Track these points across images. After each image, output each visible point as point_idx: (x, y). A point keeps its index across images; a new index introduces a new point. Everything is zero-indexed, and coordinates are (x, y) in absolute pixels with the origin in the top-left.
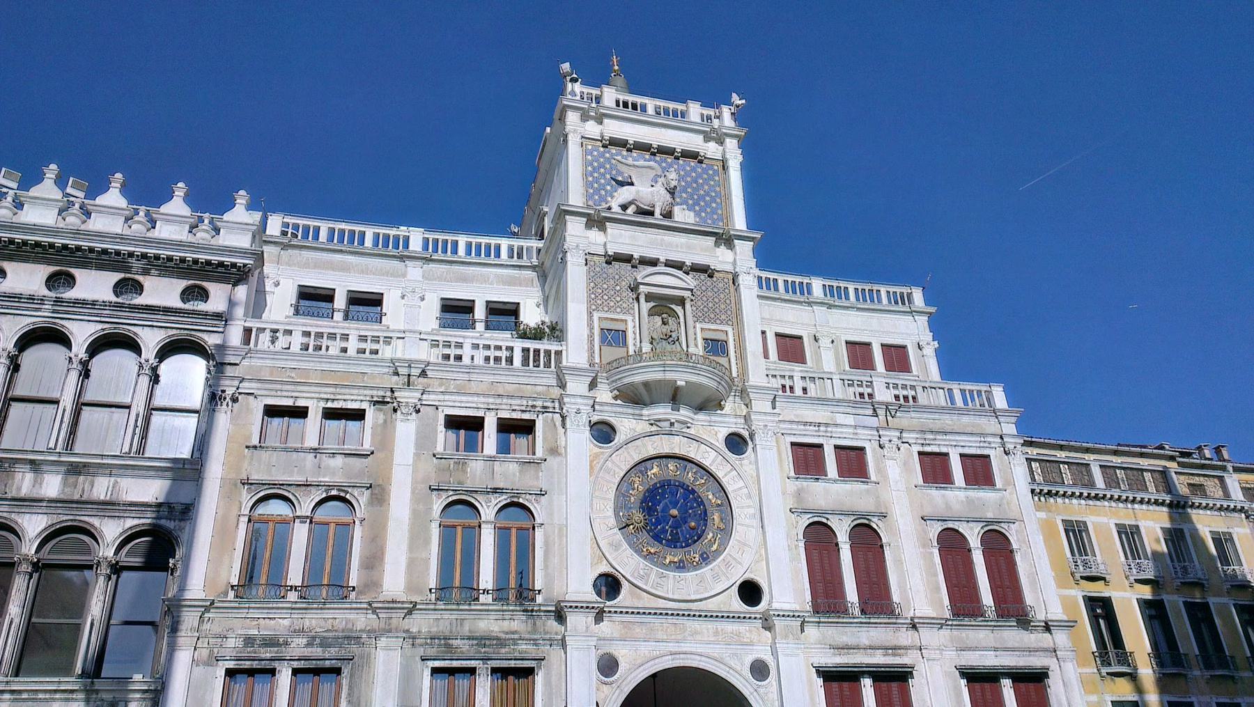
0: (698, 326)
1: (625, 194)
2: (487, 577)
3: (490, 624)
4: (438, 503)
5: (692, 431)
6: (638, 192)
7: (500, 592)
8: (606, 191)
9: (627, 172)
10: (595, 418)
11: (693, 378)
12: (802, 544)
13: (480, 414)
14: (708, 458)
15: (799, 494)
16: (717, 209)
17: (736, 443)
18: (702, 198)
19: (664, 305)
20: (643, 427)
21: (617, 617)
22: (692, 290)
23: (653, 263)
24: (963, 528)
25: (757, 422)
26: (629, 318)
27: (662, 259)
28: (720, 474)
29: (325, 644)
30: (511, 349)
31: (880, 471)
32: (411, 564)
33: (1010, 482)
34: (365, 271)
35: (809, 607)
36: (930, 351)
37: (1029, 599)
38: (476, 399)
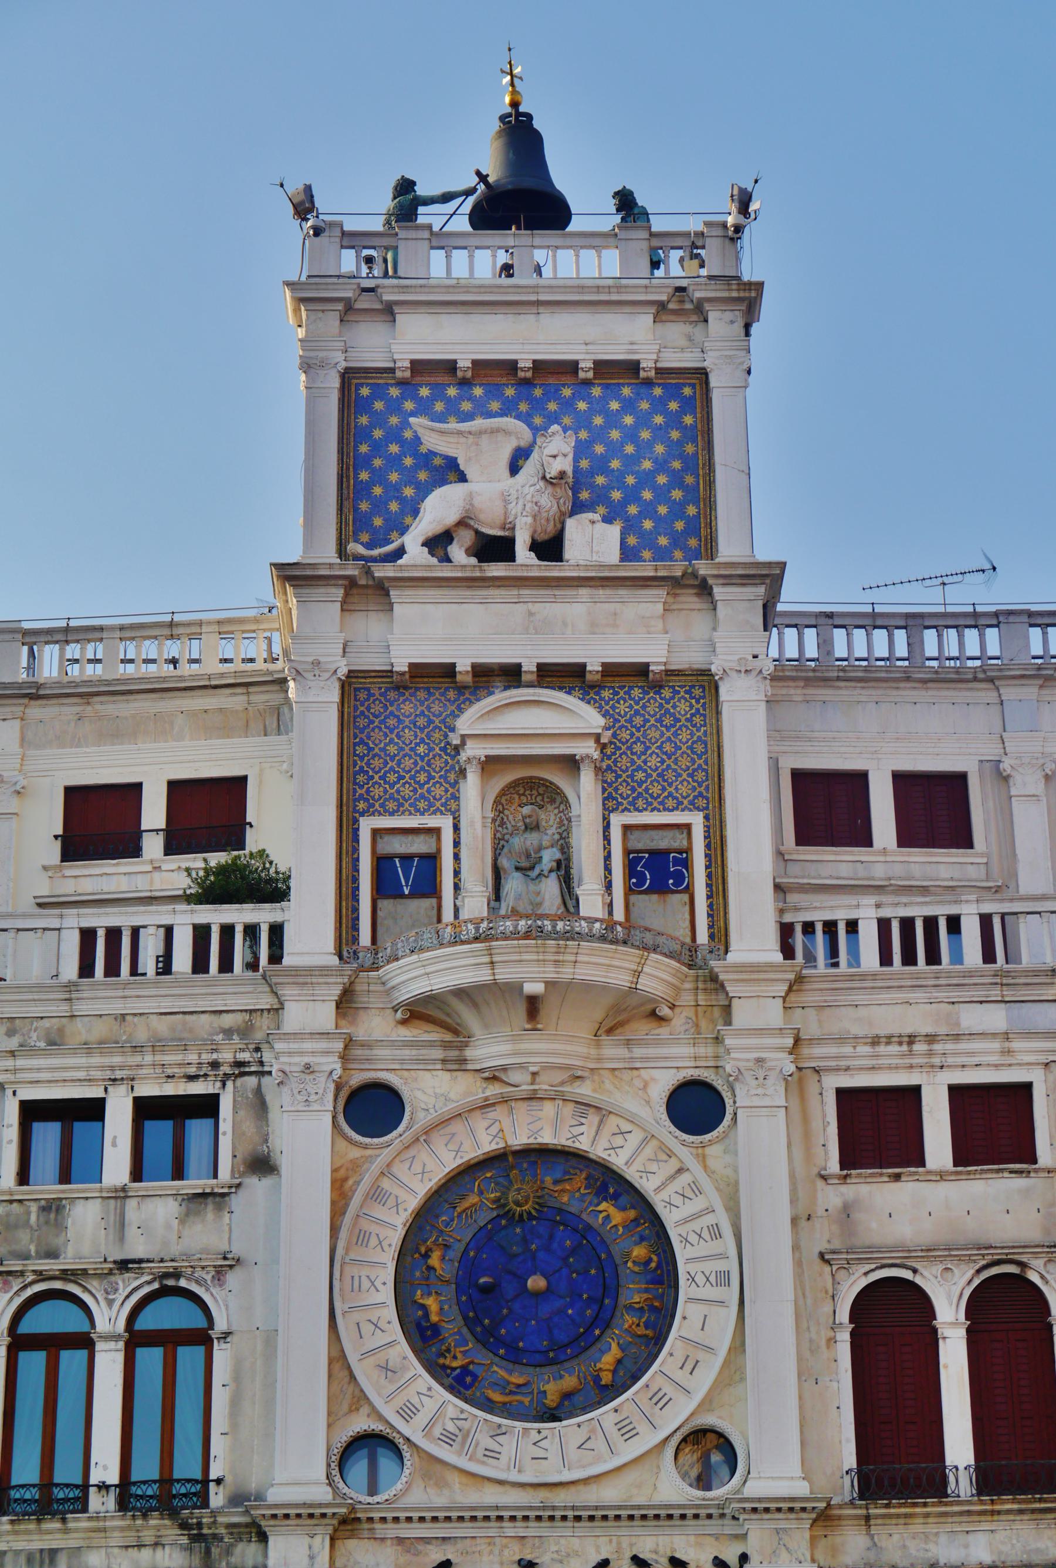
0: (617, 820)
1: (440, 508)
5: (584, 1090)
6: (471, 495)
8: (402, 500)
10: (357, 1079)
11: (567, 973)
12: (844, 1337)
13: (96, 1092)
15: (847, 1210)
16: (682, 505)
17: (697, 1107)
18: (646, 480)
19: (531, 787)
21: (392, 1531)
22: (597, 737)
23: (511, 674)
25: (739, 1051)
26: (445, 823)
27: (529, 667)
28: (647, 1186)
35: (847, 1488)
38: (82, 1061)
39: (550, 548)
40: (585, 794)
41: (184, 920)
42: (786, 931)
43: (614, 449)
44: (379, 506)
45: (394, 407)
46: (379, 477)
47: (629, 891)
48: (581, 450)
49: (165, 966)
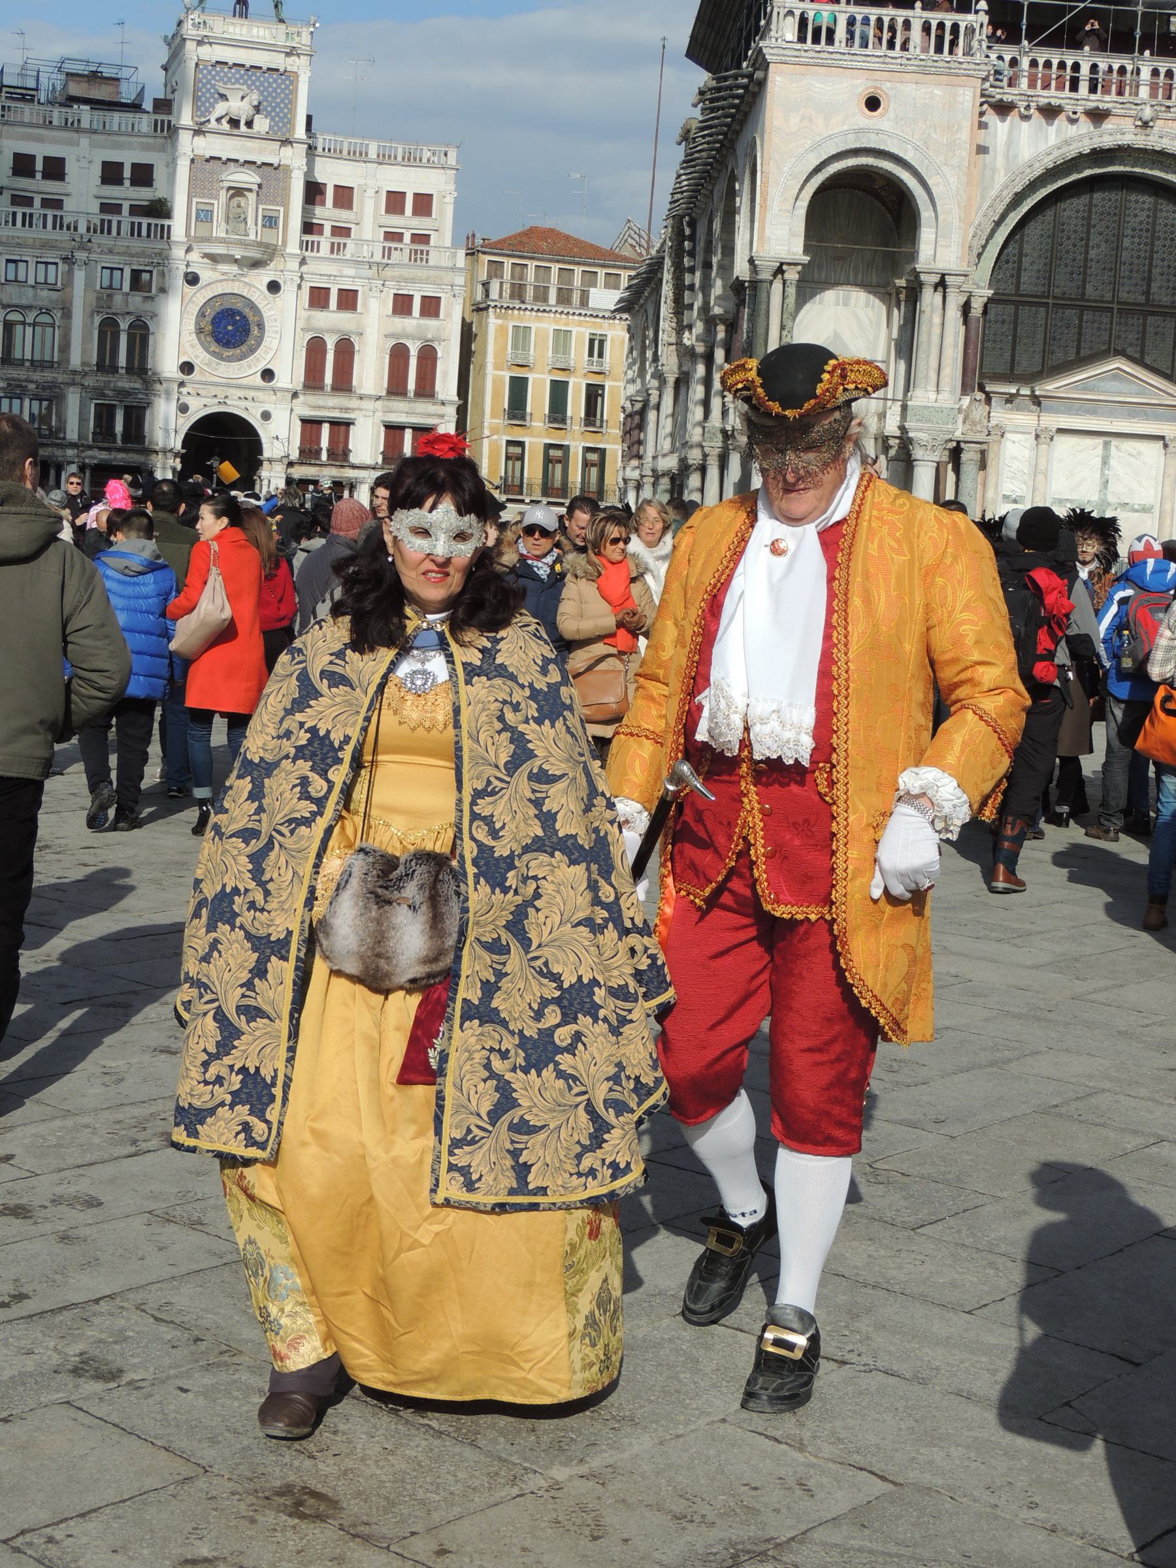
1: (221, 108)
2: (122, 360)
3: (125, 383)
4: (97, 320)
7: (130, 369)
9: (222, 91)
14: (255, 297)
15: (309, 318)
17: (274, 287)
18: (278, 105)
20: (215, 276)
24: (409, 344)
29: (44, 388)
30: (140, 224)
31: (365, 305)
32: (84, 352)
33: (449, 315)
34: (53, 141)
35: (300, 387)
36: (450, 199)
37: (438, 387)
39: (249, 124)
40: (252, 197)
41: (145, 221)
42: (302, 242)
43: (270, 94)
44: (203, 104)
45: (209, 72)
46: (204, 94)
47: (264, 226)
48: (261, 93)
49: (139, 235)
